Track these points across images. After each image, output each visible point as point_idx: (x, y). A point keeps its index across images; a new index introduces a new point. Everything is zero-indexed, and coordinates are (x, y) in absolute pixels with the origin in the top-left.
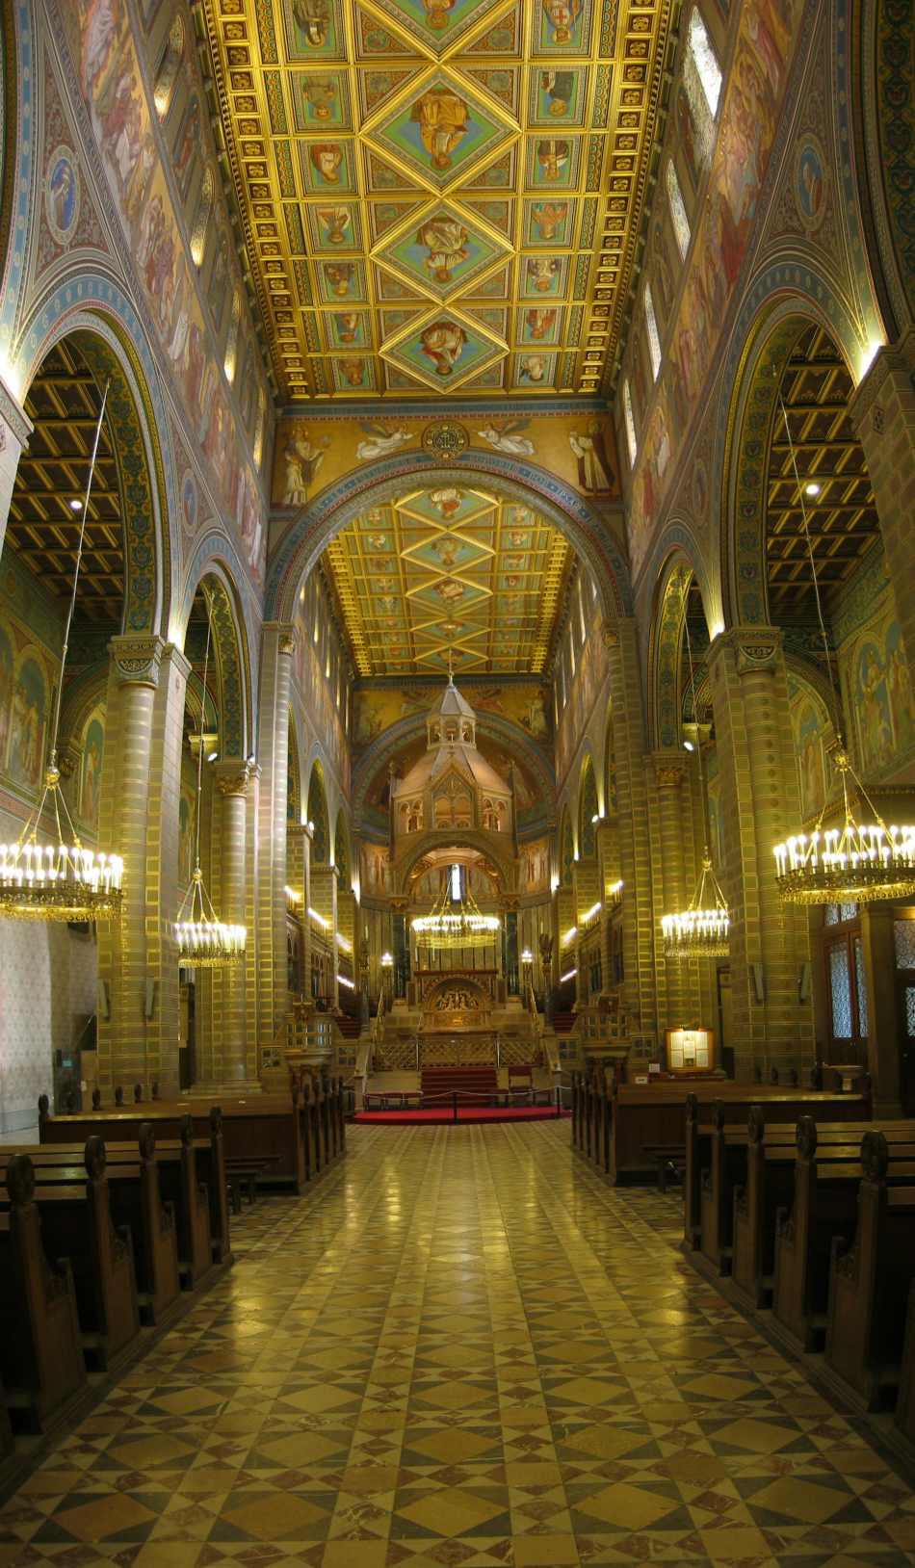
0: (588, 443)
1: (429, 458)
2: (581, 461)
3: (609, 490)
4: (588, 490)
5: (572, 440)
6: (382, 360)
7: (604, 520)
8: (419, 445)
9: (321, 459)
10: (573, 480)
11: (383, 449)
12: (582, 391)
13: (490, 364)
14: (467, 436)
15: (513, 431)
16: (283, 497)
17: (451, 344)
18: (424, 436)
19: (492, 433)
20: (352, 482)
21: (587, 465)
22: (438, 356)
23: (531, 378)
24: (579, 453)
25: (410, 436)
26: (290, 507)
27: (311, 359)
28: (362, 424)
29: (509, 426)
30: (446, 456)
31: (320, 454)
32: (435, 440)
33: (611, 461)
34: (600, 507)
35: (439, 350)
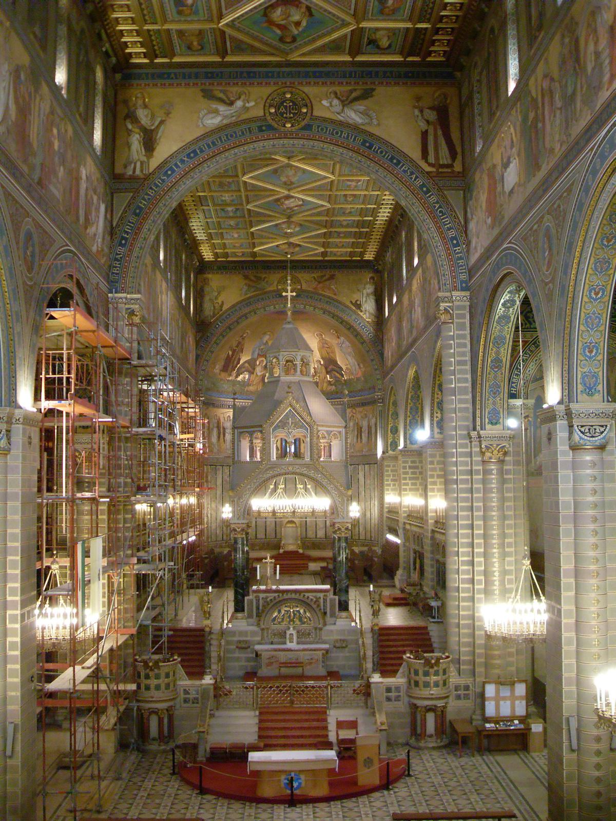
0: (432, 116)
1: (270, 128)
2: (425, 135)
3: (451, 166)
4: (430, 165)
5: (417, 112)
6: (223, 33)
7: (444, 196)
8: (261, 113)
9: (162, 128)
10: (415, 153)
11: (225, 117)
12: (429, 59)
13: (335, 35)
14: (310, 105)
15: (357, 99)
16: (125, 167)
17: (296, 18)
18: (267, 105)
19: (336, 102)
20: (194, 152)
21: (431, 139)
22: (282, 27)
23: (378, 47)
24: (423, 126)
25: (252, 104)
26: (133, 178)
27: (149, 31)
28: (202, 90)
29: (354, 95)
30: (289, 125)
31: (162, 122)
32: (277, 108)
33: (455, 135)
34: (441, 184)
35: (283, 23)
